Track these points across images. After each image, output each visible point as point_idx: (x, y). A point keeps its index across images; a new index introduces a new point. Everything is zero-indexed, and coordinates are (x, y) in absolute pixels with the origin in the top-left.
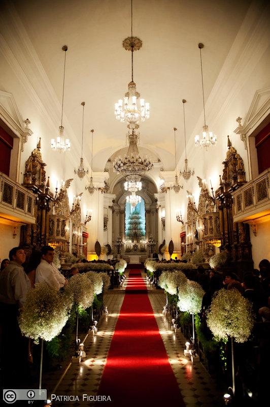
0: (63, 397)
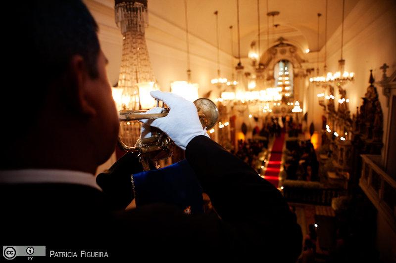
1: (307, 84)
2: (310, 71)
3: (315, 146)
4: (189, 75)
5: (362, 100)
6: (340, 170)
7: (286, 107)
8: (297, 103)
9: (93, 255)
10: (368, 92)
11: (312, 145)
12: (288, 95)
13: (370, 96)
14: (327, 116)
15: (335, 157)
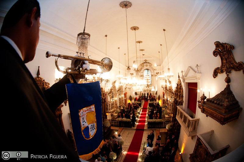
1: (157, 79)
2: (157, 73)
3: (160, 105)
5: (177, 85)
7: (149, 89)
8: (153, 87)
9: (57, 157)
10: (178, 81)
11: (159, 104)
12: (149, 84)
14: (165, 92)
15: (168, 109)
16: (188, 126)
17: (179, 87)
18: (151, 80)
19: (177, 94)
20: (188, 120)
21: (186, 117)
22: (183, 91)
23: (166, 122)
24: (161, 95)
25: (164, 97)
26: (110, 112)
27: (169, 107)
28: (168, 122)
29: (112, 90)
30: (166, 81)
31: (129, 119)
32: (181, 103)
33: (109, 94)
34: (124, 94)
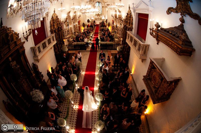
0: (31, 128)
3: (110, 31)
4: (62, 5)
6: (119, 37)
7: (99, 17)
8: (103, 16)
11: (109, 30)
12: (100, 13)
13: (129, 13)
14: (114, 20)
15: (118, 33)
16: (139, 50)
17: (129, 16)
18: (101, 10)
19: (127, 22)
20: (138, 44)
21: (136, 41)
22: (133, 19)
23: (116, 44)
24: (111, 22)
25: (113, 24)
26: (67, 38)
27: (119, 32)
28: (118, 44)
29: (68, 19)
30: (116, 11)
31: (83, 42)
32: (131, 29)
33: (64, 23)
34: (77, 22)
